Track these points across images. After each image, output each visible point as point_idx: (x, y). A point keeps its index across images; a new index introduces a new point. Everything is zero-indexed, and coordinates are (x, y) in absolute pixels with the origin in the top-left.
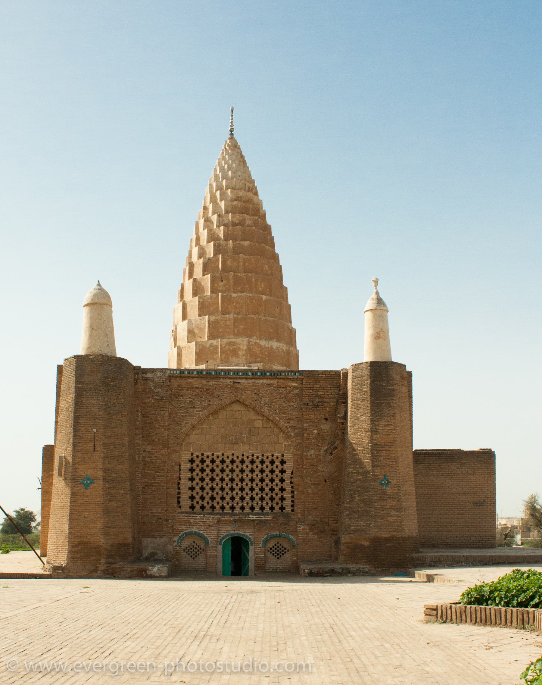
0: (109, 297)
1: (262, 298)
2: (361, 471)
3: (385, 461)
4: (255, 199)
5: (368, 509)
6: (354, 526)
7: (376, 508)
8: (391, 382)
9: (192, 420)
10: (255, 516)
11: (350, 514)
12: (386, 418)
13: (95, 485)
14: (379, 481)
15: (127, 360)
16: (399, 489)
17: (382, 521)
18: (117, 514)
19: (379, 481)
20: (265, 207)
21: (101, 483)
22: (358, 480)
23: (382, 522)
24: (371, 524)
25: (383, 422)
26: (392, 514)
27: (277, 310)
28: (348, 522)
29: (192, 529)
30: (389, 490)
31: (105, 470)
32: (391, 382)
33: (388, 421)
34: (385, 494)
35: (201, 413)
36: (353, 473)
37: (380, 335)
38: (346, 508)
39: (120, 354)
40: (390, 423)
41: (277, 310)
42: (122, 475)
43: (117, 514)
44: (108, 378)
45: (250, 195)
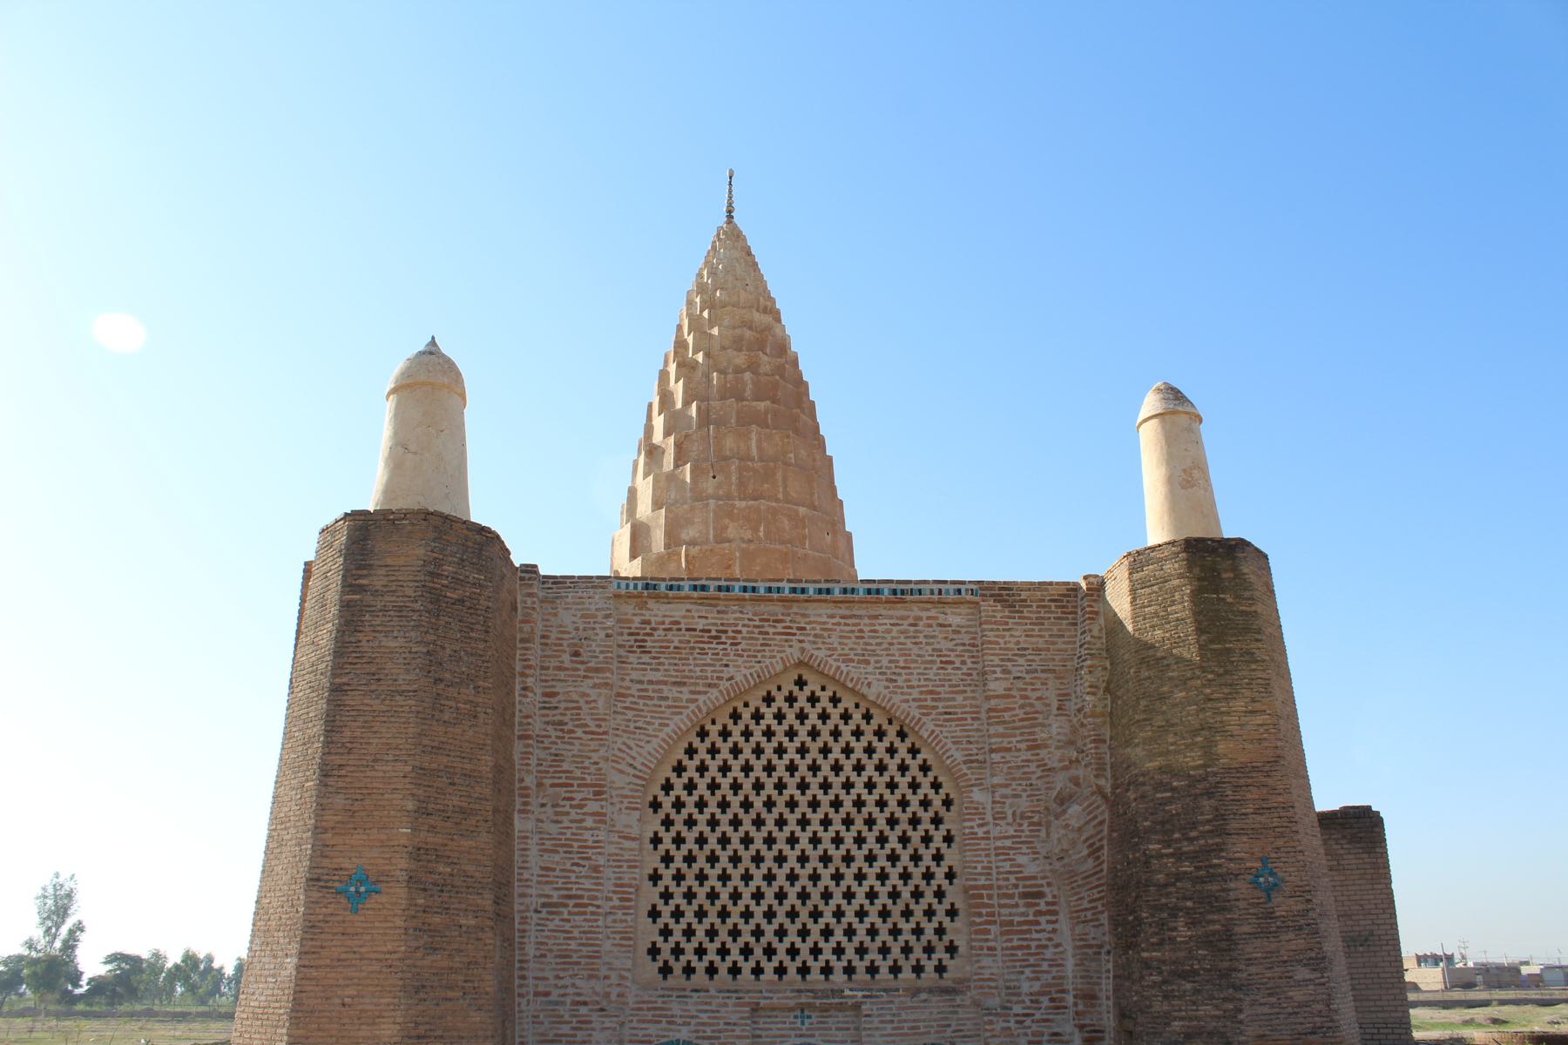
0: (458, 374)
1: (797, 512)
2: (1187, 847)
3: (1258, 818)
4: (778, 331)
5: (1226, 964)
6: (1182, 1019)
7: (1250, 961)
8: (1247, 594)
9: (677, 718)
10: (860, 994)
11: (1164, 982)
12: (1247, 693)
13: (383, 899)
14: (1250, 877)
15: (498, 537)
16: (1309, 901)
17: (1273, 1000)
18: (450, 994)
19: (1250, 877)
20: (795, 347)
21: (401, 892)
22: (1179, 877)
23: (1272, 1006)
24: (1241, 1011)
25: (1239, 705)
26: (1298, 977)
27: (829, 538)
28: (1159, 1006)
29: (678, 1036)
30: (1283, 905)
31: (418, 853)
32: (1247, 594)
33: (1253, 701)
34: (1270, 915)
35: (702, 698)
36: (1163, 856)
37: (1189, 480)
38: (1146, 964)
39: (478, 516)
40: (1258, 706)
41: (829, 538)
42: (470, 868)
43: (450, 994)
44: (439, 576)
45: (767, 319)
